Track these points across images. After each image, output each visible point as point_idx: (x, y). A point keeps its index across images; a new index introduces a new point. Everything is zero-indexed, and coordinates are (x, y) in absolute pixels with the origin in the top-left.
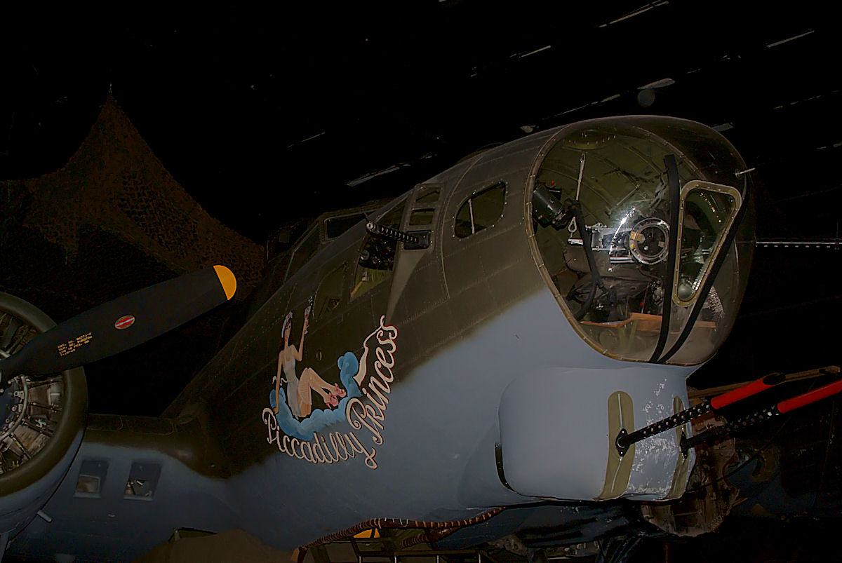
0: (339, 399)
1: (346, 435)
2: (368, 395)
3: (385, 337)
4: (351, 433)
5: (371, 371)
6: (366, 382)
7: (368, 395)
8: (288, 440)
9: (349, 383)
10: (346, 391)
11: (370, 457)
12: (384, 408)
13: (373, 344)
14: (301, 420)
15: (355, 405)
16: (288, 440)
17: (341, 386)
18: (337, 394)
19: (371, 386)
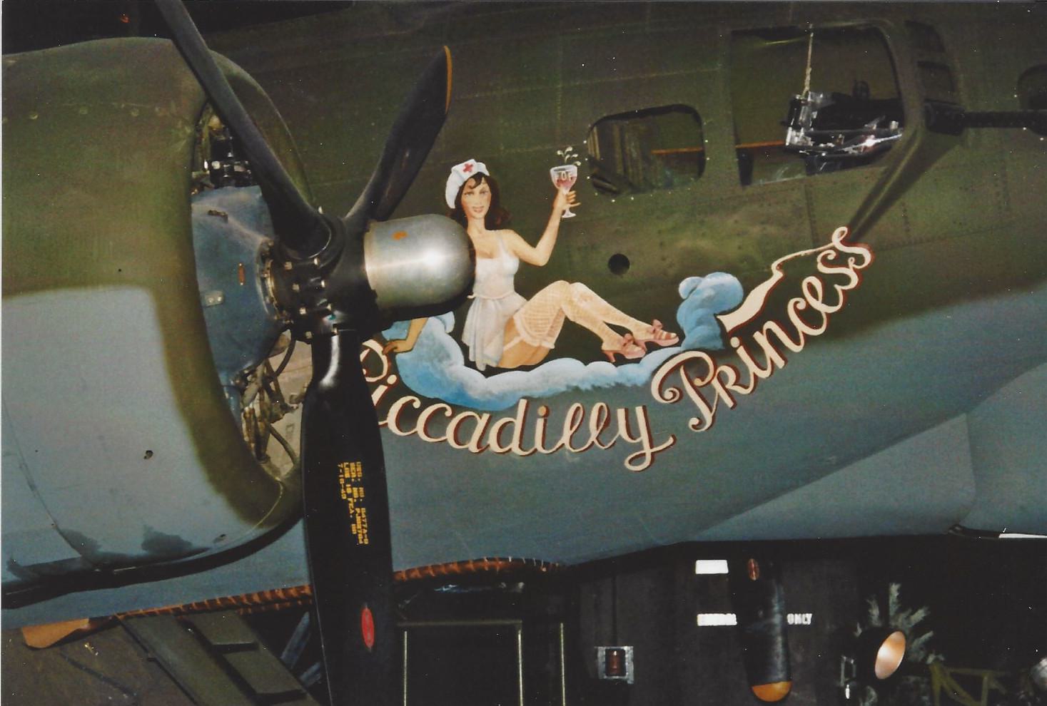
0: (651, 347)
1: (621, 413)
2: (742, 352)
3: (841, 259)
4: (639, 411)
5: (774, 308)
6: (745, 332)
7: (742, 352)
8: (417, 404)
9: (699, 322)
10: (681, 336)
11: (648, 451)
12: (764, 374)
13: (807, 266)
14: (490, 372)
15: (688, 364)
16: (417, 404)
17: (671, 325)
18: (651, 337)
19: (761, 338)
